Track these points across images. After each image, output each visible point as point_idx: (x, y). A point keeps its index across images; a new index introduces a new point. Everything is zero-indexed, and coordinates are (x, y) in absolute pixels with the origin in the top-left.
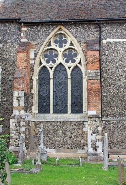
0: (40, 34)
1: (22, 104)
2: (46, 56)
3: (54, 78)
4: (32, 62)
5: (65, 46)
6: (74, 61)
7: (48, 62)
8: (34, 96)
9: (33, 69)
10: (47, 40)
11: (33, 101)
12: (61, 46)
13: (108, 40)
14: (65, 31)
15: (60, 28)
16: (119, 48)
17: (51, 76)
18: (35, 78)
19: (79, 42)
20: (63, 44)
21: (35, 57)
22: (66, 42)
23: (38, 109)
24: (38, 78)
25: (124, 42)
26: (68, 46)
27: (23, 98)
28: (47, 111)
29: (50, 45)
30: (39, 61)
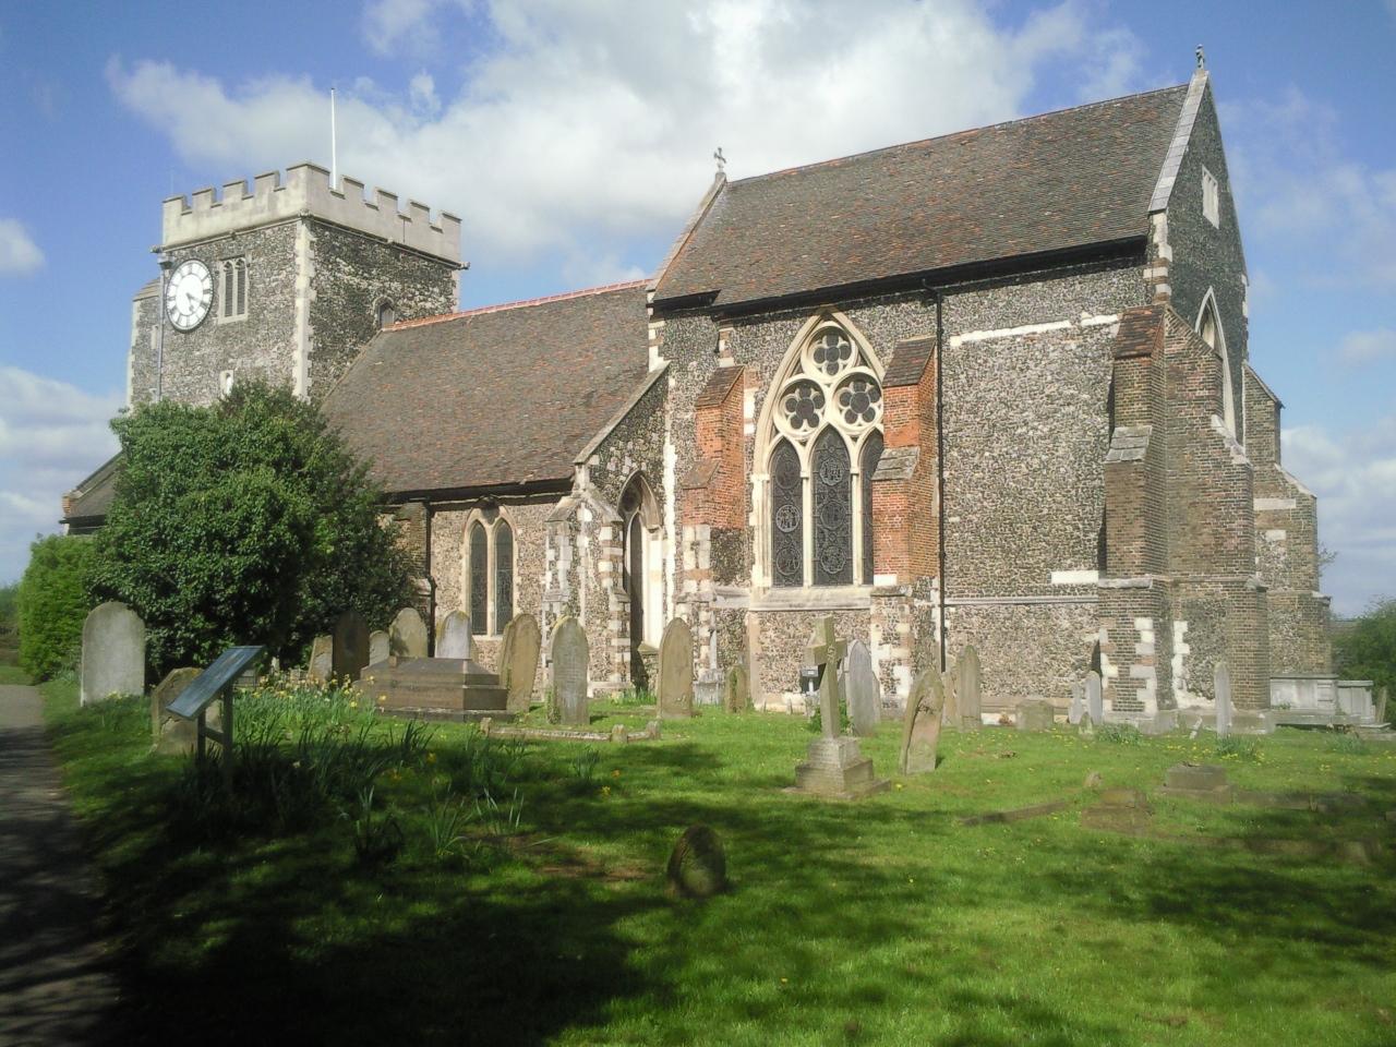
0: (768, 338)
1: (705, 564)
2: (791, 406)
3: (816, 475)
5: (845, 366)
6: (869, 416)
7: (796, 424)
8: (758, 535)
9: (753, 452)
10: (788, 355)
12: (833, 370)
13: (967, 337)
14: (843, 319)
16: (1001, 361)
17: (806, 470)
18: (760, 480)
19: (880, 353)
20: (840, 361)
22: (846, 352)
24: (767, 477)
25: (1015, 337)
26: (849, 367)
27: (707, 545)
28: (796, 579)
29: (798, 369)
30: (770, 424)
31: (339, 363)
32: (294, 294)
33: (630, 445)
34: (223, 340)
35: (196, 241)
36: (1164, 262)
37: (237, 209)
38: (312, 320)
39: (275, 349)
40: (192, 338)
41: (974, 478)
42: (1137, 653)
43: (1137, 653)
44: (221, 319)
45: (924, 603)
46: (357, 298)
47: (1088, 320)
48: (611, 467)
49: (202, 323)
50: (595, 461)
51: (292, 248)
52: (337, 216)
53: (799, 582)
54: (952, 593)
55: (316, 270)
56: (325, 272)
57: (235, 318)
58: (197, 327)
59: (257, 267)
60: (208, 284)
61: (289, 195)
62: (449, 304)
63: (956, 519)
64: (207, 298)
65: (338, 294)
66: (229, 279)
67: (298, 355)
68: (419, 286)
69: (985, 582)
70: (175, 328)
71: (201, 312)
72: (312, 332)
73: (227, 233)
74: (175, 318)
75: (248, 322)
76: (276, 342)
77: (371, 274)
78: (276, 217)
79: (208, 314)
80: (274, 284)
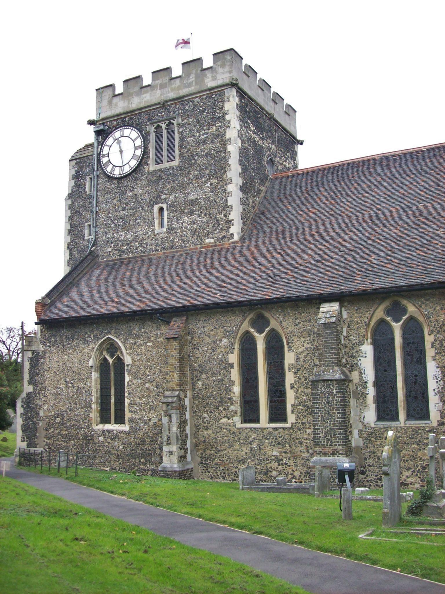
32: (225, 143)
34: (156, 181)
37: (166, 87)
38: (241, 162)
39: (208, 185)
40: (125, 183)
44: (152, 167)
46: (259, 150)
51: (222, 109)
55: (240, 125)
57: (166, 165)
58: (130, 174)
59: (187, 126)
60: (139, 142)
61: (216, 72)
62: (295, 166)
64: (139, 152)
66: (159, 138)
67: (231, 188)
68: (282, 150)
70: (109, 177)
71: (134, 163)
73: (159, 104)
74: (109, 169)
75: (178, 167)
76: (209, 180)
78: (205, 88)
79: (140, 164)
80: (203, 137)
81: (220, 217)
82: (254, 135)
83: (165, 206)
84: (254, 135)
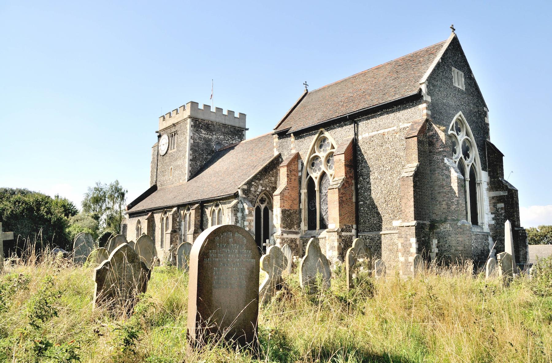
4: (300, 174)
8: (303, 211)
9: (301, 182)
11: (302, 217)
15: (322, 131)
18: (304, 191)
21: (302, 168)
23: (307, 225)
29: (315, 152)
30: (306, 172)
31: (201, 162)
33: (261, 182)
35: (165, 128)
36: (426, 102)
38: (191, 149)
41: (367, 187)
42: (411, 252)
43: (411, 252)
45: (349, 234)
47: (402, 126)
48: (252, 189)
49: (166, 153)
50: (245, 187)
52: (200, 116)
53: (315, 229)
54: (361, 230)
55: (193, 133)
56: (196, 134)
58: (165, 154)
63: (362, 203)
65: (201, 140)
68: (230, 136)
69: (371, 226)
72: (191, 153)
77: (212, 133)
81: (184, 172)
82: (204, 135)
83: (172, 167)
84: (205, 135)
